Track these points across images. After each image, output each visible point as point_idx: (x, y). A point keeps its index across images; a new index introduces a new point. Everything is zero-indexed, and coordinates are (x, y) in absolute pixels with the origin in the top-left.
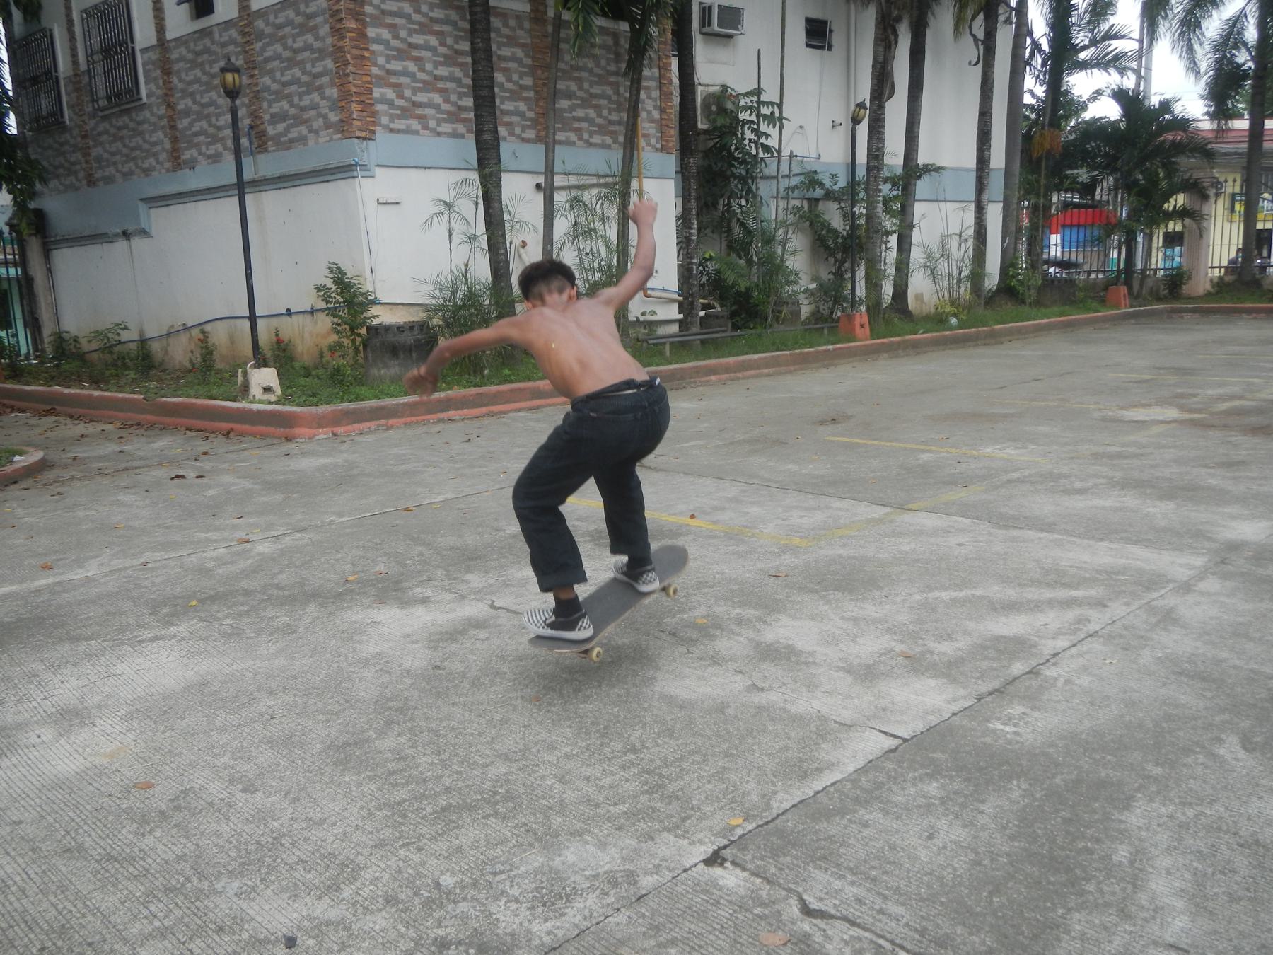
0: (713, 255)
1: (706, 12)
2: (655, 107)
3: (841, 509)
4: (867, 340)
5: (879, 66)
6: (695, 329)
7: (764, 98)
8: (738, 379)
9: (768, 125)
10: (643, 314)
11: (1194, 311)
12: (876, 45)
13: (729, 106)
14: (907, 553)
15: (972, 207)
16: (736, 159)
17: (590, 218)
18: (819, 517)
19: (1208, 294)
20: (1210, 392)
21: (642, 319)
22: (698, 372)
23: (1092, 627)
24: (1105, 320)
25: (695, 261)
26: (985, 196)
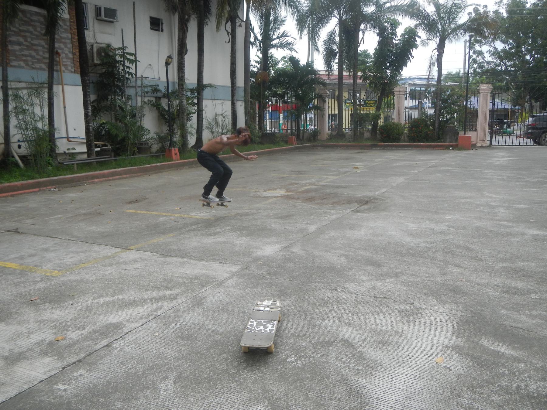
0: (105, 122)
1: (98, 10)
2: (69, 52)
3: (96, 252)
4: (178, 160)
5: (180, 40)
6: (94, 157)
7: (127, 51)
8: (110, 180)
9: (130, 63)
10: (68, 149)
11: (321, 146)
12: (179, 31)
13: (111, 54)
14: (106, 275)
15: (229, 103)
16: (116, 78)
17: (23, 104)
18: (81, 256)
19: (327, 139)
20: (304, 182)
21: (67, 152)
22: (87, 178)
23: (160, 312)
24: (286, 150)
25: (91, 125)
26: (235, 98)
